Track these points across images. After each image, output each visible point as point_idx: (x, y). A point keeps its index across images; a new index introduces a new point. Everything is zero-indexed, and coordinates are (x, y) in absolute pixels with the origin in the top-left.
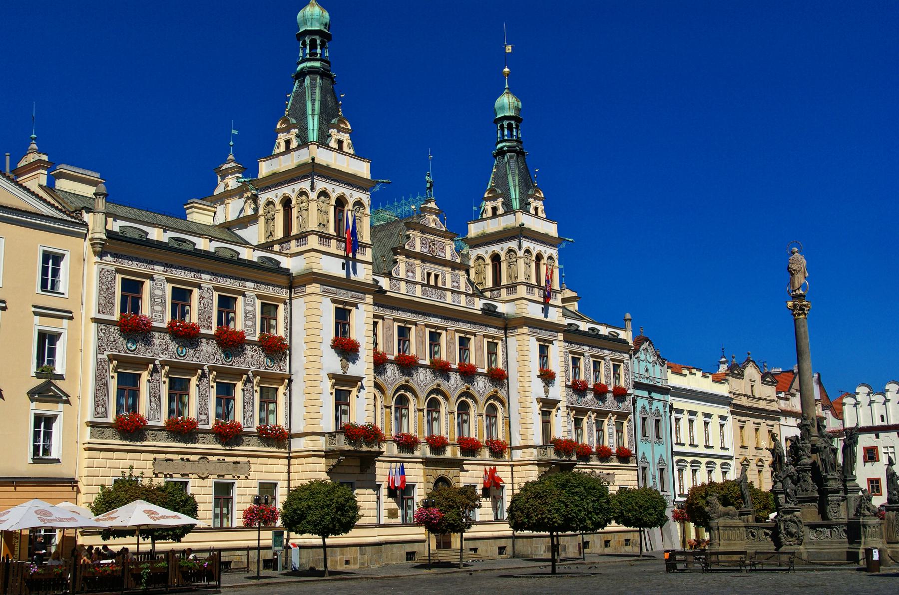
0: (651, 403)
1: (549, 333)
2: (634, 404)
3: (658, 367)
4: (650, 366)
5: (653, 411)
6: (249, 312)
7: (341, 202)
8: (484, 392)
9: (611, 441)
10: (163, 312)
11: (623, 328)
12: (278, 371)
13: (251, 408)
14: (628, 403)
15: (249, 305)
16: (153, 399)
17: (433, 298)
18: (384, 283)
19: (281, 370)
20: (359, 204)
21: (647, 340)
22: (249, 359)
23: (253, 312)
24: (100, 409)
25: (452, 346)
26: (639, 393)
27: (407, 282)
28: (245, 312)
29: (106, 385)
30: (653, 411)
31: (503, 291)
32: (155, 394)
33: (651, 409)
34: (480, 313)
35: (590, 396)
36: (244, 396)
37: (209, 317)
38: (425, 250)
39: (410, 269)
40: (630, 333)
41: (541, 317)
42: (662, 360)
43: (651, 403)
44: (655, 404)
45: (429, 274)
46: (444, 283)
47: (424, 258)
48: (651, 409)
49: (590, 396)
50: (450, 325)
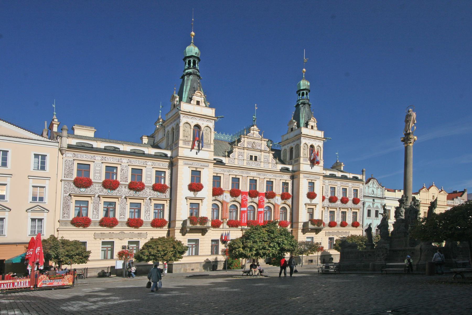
0: (373, 204)
2: (363, 205)
3: (379, 190)
4: (375, 190)
5: (375, 207)
6: (149, 175)
10: (100, 176)
14: (360, 204)
16: (95, 211)
18: (225, 160)
21: (373, 178)
22: (148, 193)
24: (65, 215)
25: (262, 185)
26: (366, 200)
27: (238, 159)
28: (147, 175)
29: (69, 206)
30: (375, 207)
31: (293, 161)
33: (373, 207)
35: (339, 202)
38: (249, 146)
39: (240, 154)
40: (364, 177)
42: (381, 185)
43: (373, 204)
44: (375, 206)
45: (251, 157)
46: (260, 160)
47: (248, 149)
48: (373, 207)
49: (339, 202)
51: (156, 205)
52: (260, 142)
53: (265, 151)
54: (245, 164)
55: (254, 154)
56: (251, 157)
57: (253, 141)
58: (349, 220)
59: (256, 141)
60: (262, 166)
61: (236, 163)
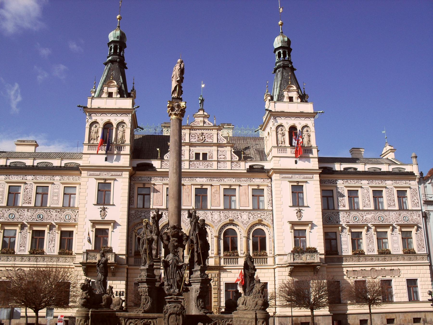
1: (302, 176)
7: (108, 126)
9: (396, 246)
11: (411, 164)
12: (73, 222)
13: (53, 243)
15: (56, 189)
19: (75, 221)
20: (121, 123)
22: (54, 217)
23: (58, 193)
25: (217, 196)
32: (370, 239)
34: (246, 171)
36: (49, 236)
37: (30, 198)
41: (294, 166)
45: (197, 155)
50: (215, 182)
51: (62, 233)
52: (209, 132)
53: (219, 145)
55: (201, 150)
56: (197, 155)
59: (205, 132)
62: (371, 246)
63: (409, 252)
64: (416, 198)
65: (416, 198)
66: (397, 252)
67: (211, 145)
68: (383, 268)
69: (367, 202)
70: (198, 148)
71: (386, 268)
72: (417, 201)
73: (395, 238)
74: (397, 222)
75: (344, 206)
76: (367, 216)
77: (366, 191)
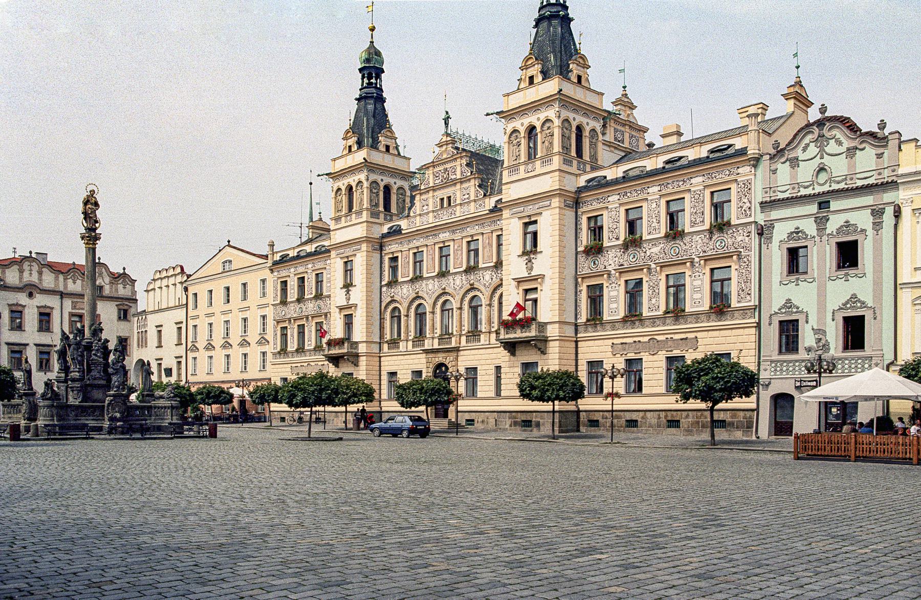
8: (490, 284)
17: (445, 217)
47: (434, 189)
54: (431, 220)
55: (444, 193)
57: (441, 168)
58: (698, 297)
60: (459, 213)
61: (419, 223)
62: (654, 301)
63: (720, 305)
64: (746, 201)
65: (746, 201)
66: (697, 306)
67: (454, 183)
68: (669, 336)
69: (655, 224)
70: (442, 191)
71: (676, 337)
72: (748, 204)
73: (697, 283)
74: (705, 252)
75: (617, 239)
76: (652, 250)
77: (654, 205)
